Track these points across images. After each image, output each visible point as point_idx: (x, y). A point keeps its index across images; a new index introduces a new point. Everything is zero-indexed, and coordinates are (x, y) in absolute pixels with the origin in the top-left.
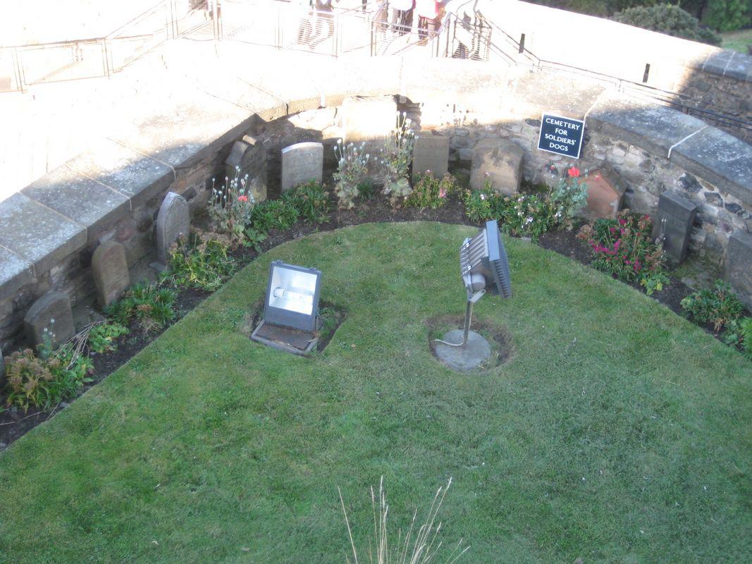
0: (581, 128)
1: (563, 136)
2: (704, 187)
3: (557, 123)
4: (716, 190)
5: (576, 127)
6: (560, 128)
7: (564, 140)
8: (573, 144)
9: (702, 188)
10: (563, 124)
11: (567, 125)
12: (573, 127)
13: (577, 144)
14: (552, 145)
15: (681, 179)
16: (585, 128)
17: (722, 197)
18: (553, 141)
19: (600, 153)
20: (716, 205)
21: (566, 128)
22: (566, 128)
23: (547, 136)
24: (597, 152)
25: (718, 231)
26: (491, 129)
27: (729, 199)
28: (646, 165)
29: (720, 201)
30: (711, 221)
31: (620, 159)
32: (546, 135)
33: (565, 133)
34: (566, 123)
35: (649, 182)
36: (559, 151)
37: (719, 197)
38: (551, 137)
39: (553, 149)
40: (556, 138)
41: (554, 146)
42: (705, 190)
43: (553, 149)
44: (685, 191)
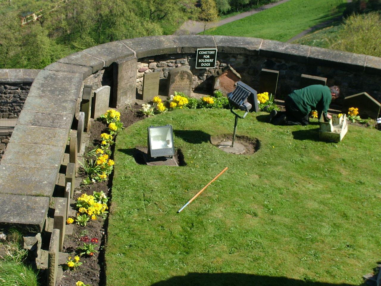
0: (215, 53)
1: (207, 59)
2: (277, 63)
3: (204, 53)
4: (283, 62)
6: (205, 55)
7: (208, 61)
9: (275, 64)
10: (207, 53)
11: (209, 52)
12: (212, 53)
13: (214, 61)
15: (264, 63)
17: (287, 64)
18: (203, 62)
20: (284, 70)
21: (209, 54)
33: (208, 56)
34: (208, 52)
39: (203, 66)
40: (204, 61)
42: (277, 64)
43: (203, 66)
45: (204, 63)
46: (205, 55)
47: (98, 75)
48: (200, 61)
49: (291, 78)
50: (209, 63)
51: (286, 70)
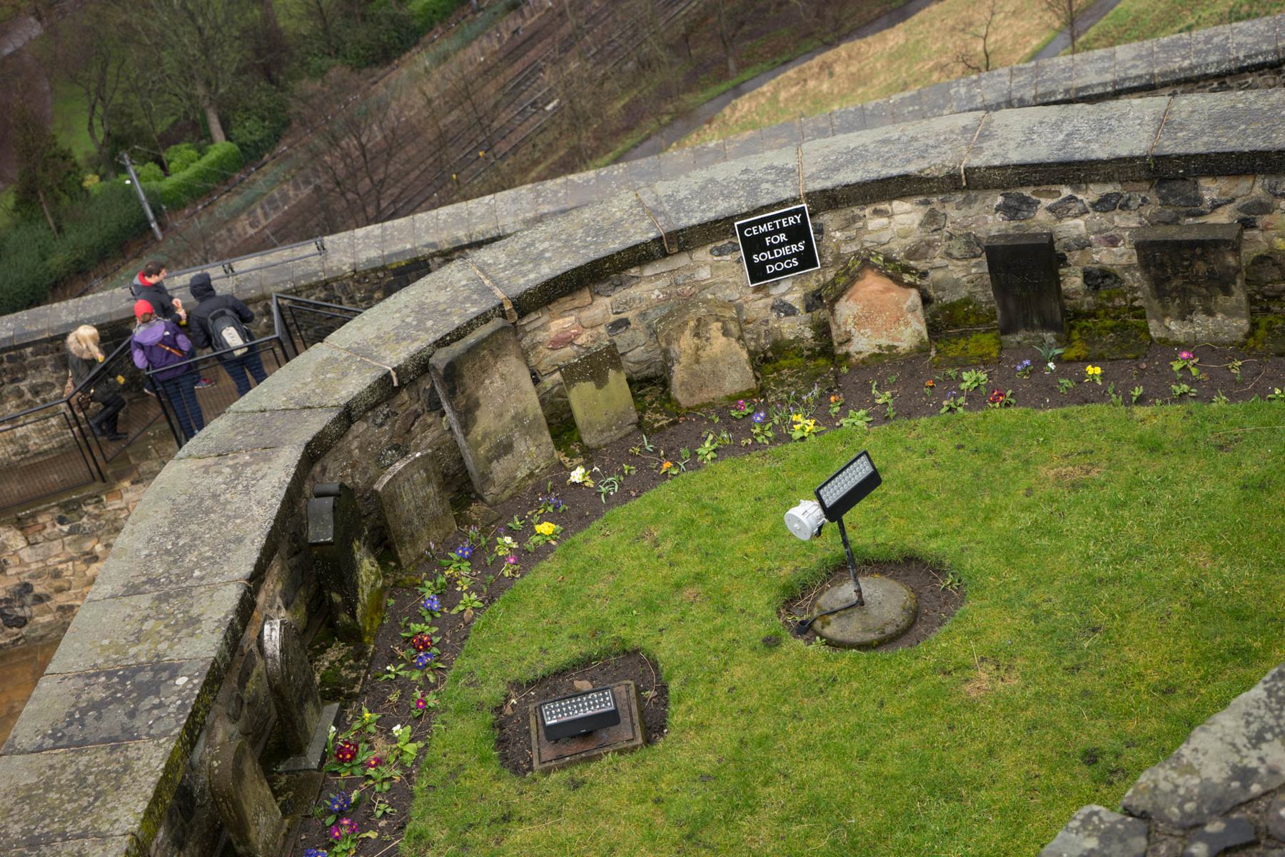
0: (804, 219)
1: (781, 245)
2: (1043, 200)
6: (769, 234)
7: (785, 251)
10: (774, 225)
11: (781, 223)
12: (791, 221)
13: (809, 245)
14: (770, 269)
15: (997, 210)
17: (1080, 197)
18: (768, 262)
19: (850, 240)
20: (1076, 216)
21: (782, 230)
22: (782, 230)
23: (756, 258)
25: (1104, 256)
28: (932, 218)
29: (1080, 205)
30: (1083, 245)
33: (782, 237)
36: (786, 272)
39: (776, 274)
40: (772, 254)
41: (775, 268)
42: (1046, 202)
43: (776, 274)
44: (1013, 223)
45: (773, 262)
46: (769, 234)
48: (757, 259)
49: (1113, 242)
50: (790, 257)
51: (1087, 216)
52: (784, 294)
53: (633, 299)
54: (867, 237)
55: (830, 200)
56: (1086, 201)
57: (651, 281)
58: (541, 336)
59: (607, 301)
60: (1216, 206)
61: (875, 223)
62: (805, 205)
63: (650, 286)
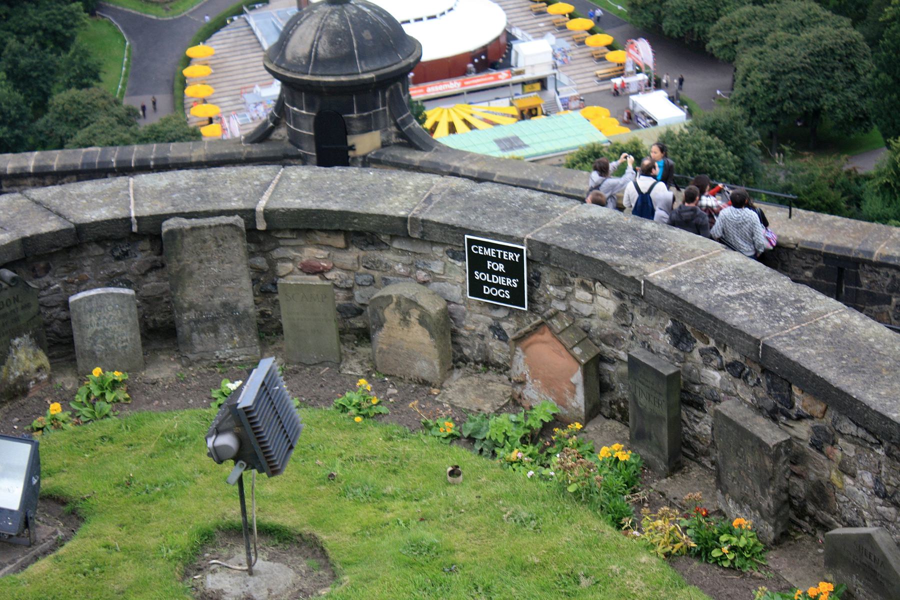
0: (521, 258)
1: (499, 274)
5: (514, 257)
7: (501, 280)
8: (516, 286)
9: (695, 342)
10: (497, 253)
11: (502, 254)
12: (511, 257)
16: (527, 258)
18: (486, 283)
23: (478, 276)
24: (556, 298)
26: (402, 271)
27: (728, 356)
28: (622, 311)
31: (586, 306)
32: (476, 273)
33: (501, 267)
34: (499, 251)
35: (630, 341)
37: (718, 353)
38: (483, 276)
39: (489, 297)
40: (491, 278)
41: (490, 291)
42: (700, 345)
43: (489, 297)
44: (675, 351)
45: (491, 285)
47: (126, 254)
52: (502, 319)
53: (380, 262)
54: (573, 303)
55: (543, 254)
56: (724, 359)
57: (398, 254)
58: (292, 253)
59: (362, 253)
60: (800, 418)
61: (581, 294)
62: (524, 248)
63: (397, 258)
